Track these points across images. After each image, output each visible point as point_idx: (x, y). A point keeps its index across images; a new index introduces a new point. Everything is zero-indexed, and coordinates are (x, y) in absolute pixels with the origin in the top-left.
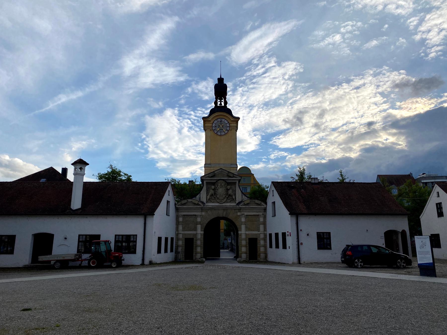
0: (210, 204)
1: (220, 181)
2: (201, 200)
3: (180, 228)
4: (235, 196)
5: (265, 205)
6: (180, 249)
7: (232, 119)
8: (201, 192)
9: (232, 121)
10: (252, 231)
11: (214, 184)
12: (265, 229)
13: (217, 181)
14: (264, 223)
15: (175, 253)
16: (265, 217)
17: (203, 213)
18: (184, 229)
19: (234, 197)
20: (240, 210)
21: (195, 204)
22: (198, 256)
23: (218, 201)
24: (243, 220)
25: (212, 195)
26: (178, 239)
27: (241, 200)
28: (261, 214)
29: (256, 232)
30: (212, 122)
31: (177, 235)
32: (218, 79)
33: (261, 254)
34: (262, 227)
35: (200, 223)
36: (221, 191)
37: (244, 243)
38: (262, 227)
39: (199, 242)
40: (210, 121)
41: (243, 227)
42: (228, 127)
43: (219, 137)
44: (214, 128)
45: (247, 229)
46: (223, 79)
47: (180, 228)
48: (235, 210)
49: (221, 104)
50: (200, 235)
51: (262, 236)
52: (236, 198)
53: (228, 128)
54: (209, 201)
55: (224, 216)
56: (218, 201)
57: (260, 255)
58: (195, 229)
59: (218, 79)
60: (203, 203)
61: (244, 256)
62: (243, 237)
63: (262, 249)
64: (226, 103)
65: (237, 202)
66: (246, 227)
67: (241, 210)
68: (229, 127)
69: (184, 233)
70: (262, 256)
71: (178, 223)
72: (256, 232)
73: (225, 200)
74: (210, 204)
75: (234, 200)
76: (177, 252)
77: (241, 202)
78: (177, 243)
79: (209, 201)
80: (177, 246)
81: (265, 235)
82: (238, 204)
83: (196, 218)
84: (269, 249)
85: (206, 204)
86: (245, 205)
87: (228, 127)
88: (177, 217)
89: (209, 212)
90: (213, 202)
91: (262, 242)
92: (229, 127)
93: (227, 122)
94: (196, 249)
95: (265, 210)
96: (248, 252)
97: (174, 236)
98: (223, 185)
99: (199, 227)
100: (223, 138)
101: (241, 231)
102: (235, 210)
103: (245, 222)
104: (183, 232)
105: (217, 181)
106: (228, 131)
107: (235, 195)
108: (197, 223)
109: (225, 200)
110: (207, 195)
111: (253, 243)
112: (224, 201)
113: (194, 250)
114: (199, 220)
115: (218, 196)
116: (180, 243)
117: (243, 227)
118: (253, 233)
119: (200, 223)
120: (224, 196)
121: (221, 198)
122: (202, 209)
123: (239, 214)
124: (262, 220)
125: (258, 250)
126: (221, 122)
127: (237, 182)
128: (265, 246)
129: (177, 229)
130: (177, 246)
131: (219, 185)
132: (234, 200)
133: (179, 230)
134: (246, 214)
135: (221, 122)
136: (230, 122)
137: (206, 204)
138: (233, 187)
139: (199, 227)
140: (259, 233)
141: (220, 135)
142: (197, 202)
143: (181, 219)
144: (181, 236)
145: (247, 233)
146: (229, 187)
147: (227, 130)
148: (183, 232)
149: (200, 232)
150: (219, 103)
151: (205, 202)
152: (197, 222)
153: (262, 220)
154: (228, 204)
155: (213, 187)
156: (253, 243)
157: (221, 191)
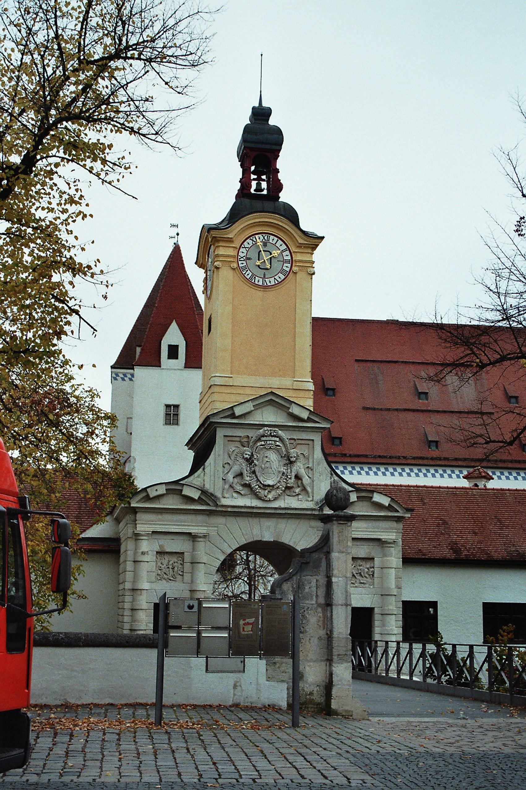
8: (207, 463)
32: (254, 108)
40: (230, 240)
44: (242, 264)
49: (259, 189)
59: (254, 108)
68: (292, 261)
92: (292, 261)
93: (284, 247)
106: (287, 276)
136: (293, 249)
141: (265, 288)
147: (282, 271)
150: (254, 184)
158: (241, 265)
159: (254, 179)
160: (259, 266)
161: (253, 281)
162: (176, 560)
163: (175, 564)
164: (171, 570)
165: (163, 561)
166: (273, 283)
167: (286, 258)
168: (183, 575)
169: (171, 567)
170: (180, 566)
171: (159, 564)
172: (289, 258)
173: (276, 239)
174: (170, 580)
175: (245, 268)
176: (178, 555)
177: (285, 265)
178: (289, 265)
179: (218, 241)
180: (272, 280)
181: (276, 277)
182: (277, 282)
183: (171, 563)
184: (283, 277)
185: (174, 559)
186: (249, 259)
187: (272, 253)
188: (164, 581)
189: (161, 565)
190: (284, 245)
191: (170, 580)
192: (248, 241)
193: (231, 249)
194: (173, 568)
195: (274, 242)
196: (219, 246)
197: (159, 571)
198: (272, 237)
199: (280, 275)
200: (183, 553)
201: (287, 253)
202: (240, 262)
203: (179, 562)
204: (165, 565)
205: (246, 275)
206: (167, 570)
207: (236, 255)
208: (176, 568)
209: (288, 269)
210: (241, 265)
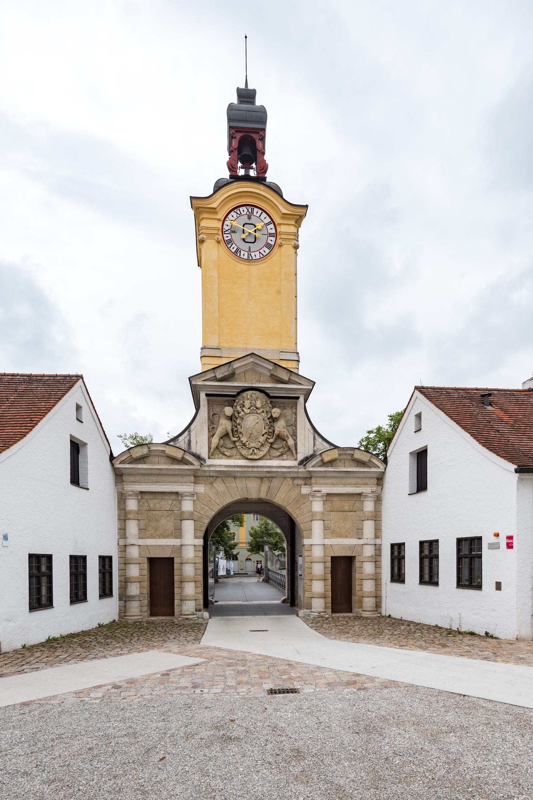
0: (220, 463)
1: (250, 392)
2: (193, 450)
3: (132, 527)
4: (295, 440)
5: (382, 466)
6: (134, 590)
7: (284, 211)
9: (285, 216)
10: (341, 536)
11: (231, 399)
12: (378, 532)
13: (239, 394)
14: (376, 517)
15: (120, 599)
16: (378, 500)
17: (201, 489)
18: (143, 532)
19: (291, 442)
20: (308, 479)
21: (174, 460)
22: (189, 607)
23: (244, 452)
24: (318, 506)
25: (226, 435)
26: (125, 562)
27: (311, 452)
28: (367, 490)
29: (353, 541)
30: (221, 216)
31: (123, 549)
32: (238, 90)
33: (366, 600)
34: (369, 527)
35: (191, 517)
36: (253, 423)
37: (318, 569)
38: (369, 527)
39: (189, 569)
40: (213, 211)
41: (317, 527)
42: (271, 235)
43: (242, 267)
44: (227, 237)
45: (328, 531)
46: (254, 91)
47: (132, 527)
48: (294, 478)
50: (192, 549)
51: (369, 551)
52: (296, 445)
53: (271, 240)
54: (216, 451)
55: (263, 495)
56: (244, 452)
57: (361, 602)
58: (178, 533)
59: (238, 90)
60: (198, 457)
61: (319, 605)
62: (318, 553)
63: (368, 586)
64: (263, 169)
65: (300, 457)
66: (326, 528)
67: (313, 480)
68: (275, 235)
69: (145, 544)
70: (369, 602)
71: (124, 516)
72: (353, 541)
73: (266, 449)
74: (220, 463)
75: (291, 451)
76: (124, 598)
77: (313, 456)
78: (123, 570)
79: (216, 451)
80: (125, 582)
81: (378, 549)
82: (301, 463)
83: (180, 502)
84: (389, 588)
85: (209, 462)
86: (324, 464)
87: (271, 235)
88: (122, 498)
89: (219, 485)
90: (229, 457)
91: (368, 568)
92: (275, 235)
93: (268, 220)
94: (181, 588)
95: (380, 479)
96: (329, 594)
97: (113, 552)
98: (259, 404)
99: (188, 526)
100: (255, 269)
101: (310, 537)
102: (294, 478)
103: (323, 513)
104: (141, 542)
105: (239, 394)
107: (294, 435)
108: (182, 517)
109: (266, 449)
110: (211, 436)
111: (342, 569)
112: (262, 454)
113: (176, 590)
114: (187, 506)
115: (244, 439)
116: (134, 571)
117: (317, 527)
118: (342, 545)
119: (191, 517)
120: (262, 439)
121: (252, 445)
122: (197, 477)
123: (305, 490)
124: (369, 506)
125: (357, 588)
126: (249, 218)
127: (302, 399)
128: (377, 579)
129: (123, 532)
130: (125, 582)
131: (247, 403)
132: (291, 451)
133: (128, 534)
134: (325, 490)
135: (249, 218)
136: (277, 220)
137: (209, 462)
138: (288, 412)
139: (188, 526)
140: (361, 542)
141: (249, 260)
142: (179, 454)
143: (132, 505)
144: (134, 553)
145: (328, 542)
146: (276, 412)
148: (141, 542)
149: (189, 542)
151: (204, 454)
152: (182, 513)
153: (369, 506)
154: (275, 463)
155: (228, 411)
156: (342, 569)
157: (253, 423)
158: (226, 239)
159: (242, 168)
160: (244, 239)
161: (238, 255)
166: (258, 257)
167: (270, 231)
172: (273, 231)
173: (260, 211)
175: (230, 241)
177: (270, 238)
178: (274, 239)
179: (202, 212)
180: (257, 253)
181: (261, 251)
182: (262, 256)
184: (268, 251)
186: (234, 232)
187: (257, 225)
190: (268, 217)
192: (233, 213)
193: (216, 221)
195: (258, 215)
196: (203, 218)
198: (256, 210)
199: (265, 249)
201: (272, 226)
202: (225, 235)
205: (231, 249)
207: (221, 228)
209: (273, 243)
210: (226, 239)
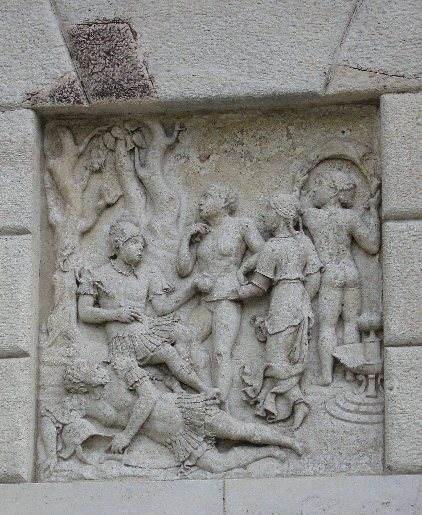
162: (286, 201)
163: (287, 247)
164: (228, 314)
165: (134, 218)
168: (375, 378)
169: (227, 282)
170: (344, 268)
171: (88, 260)
174: (223, 442)
176: (314, 141)
183: (226, 236)
185: (258, 187)
188: (146, 456)
189: (110, 276)
191: (223, 442)
194: (257, 299)
197: (89, 352)
200: (369, 104)
203: (331, 220)
204: (155, 274)
206: (190, 324)
208: (290, 304)
